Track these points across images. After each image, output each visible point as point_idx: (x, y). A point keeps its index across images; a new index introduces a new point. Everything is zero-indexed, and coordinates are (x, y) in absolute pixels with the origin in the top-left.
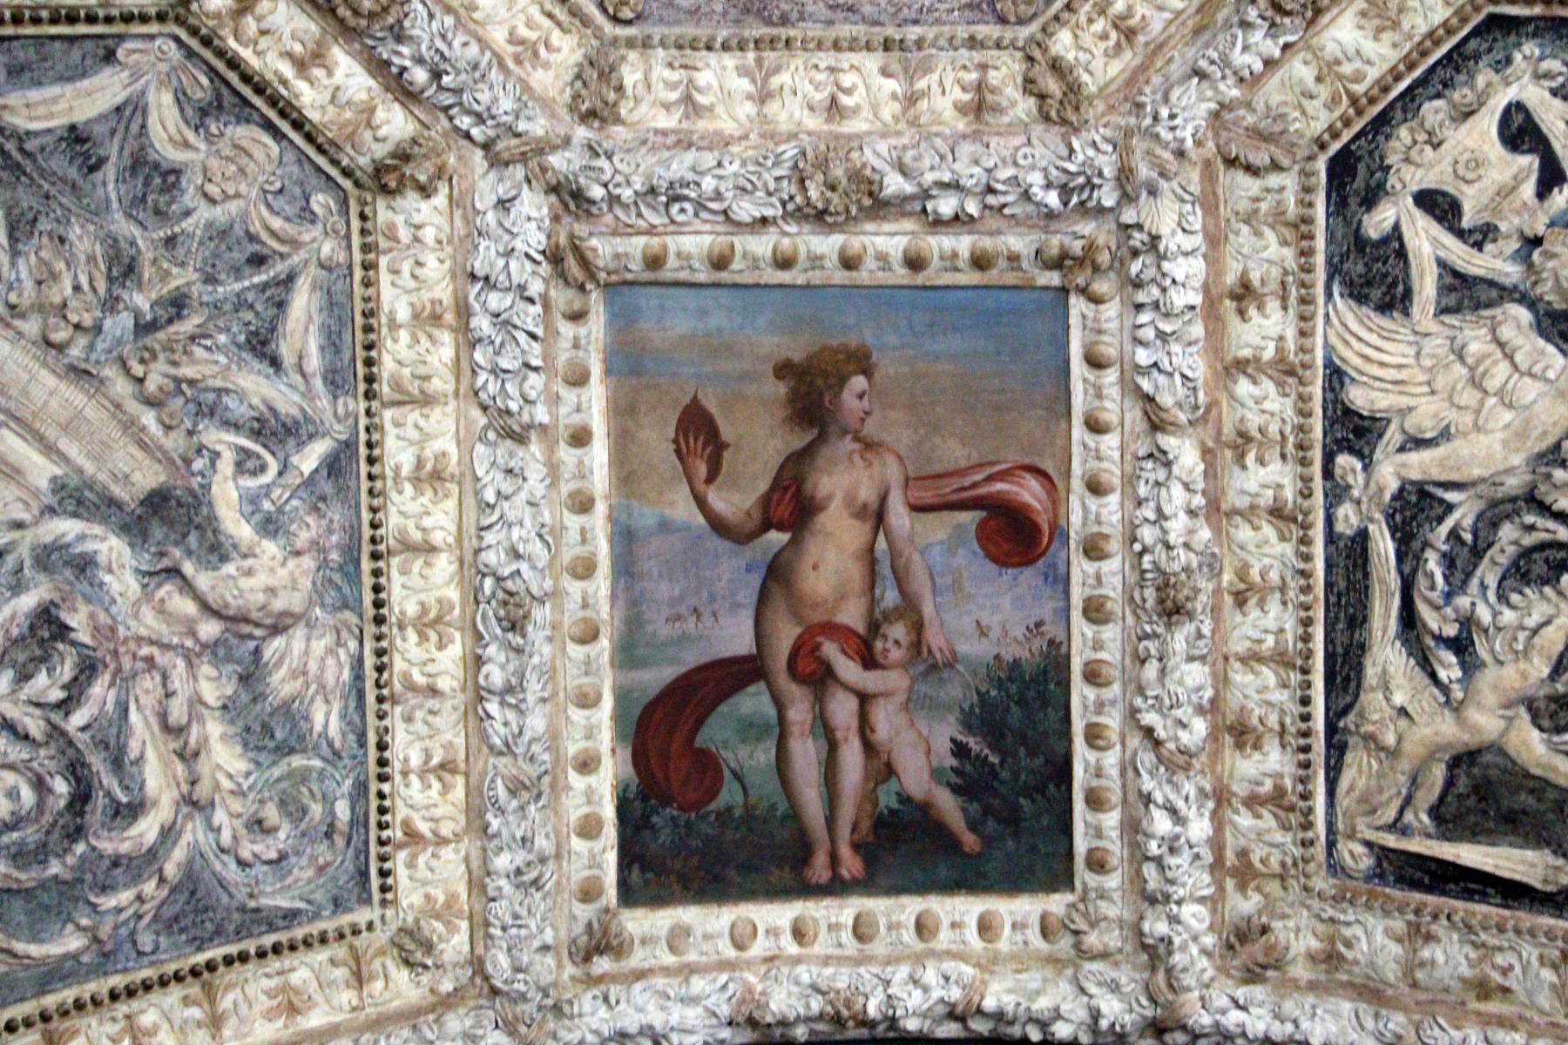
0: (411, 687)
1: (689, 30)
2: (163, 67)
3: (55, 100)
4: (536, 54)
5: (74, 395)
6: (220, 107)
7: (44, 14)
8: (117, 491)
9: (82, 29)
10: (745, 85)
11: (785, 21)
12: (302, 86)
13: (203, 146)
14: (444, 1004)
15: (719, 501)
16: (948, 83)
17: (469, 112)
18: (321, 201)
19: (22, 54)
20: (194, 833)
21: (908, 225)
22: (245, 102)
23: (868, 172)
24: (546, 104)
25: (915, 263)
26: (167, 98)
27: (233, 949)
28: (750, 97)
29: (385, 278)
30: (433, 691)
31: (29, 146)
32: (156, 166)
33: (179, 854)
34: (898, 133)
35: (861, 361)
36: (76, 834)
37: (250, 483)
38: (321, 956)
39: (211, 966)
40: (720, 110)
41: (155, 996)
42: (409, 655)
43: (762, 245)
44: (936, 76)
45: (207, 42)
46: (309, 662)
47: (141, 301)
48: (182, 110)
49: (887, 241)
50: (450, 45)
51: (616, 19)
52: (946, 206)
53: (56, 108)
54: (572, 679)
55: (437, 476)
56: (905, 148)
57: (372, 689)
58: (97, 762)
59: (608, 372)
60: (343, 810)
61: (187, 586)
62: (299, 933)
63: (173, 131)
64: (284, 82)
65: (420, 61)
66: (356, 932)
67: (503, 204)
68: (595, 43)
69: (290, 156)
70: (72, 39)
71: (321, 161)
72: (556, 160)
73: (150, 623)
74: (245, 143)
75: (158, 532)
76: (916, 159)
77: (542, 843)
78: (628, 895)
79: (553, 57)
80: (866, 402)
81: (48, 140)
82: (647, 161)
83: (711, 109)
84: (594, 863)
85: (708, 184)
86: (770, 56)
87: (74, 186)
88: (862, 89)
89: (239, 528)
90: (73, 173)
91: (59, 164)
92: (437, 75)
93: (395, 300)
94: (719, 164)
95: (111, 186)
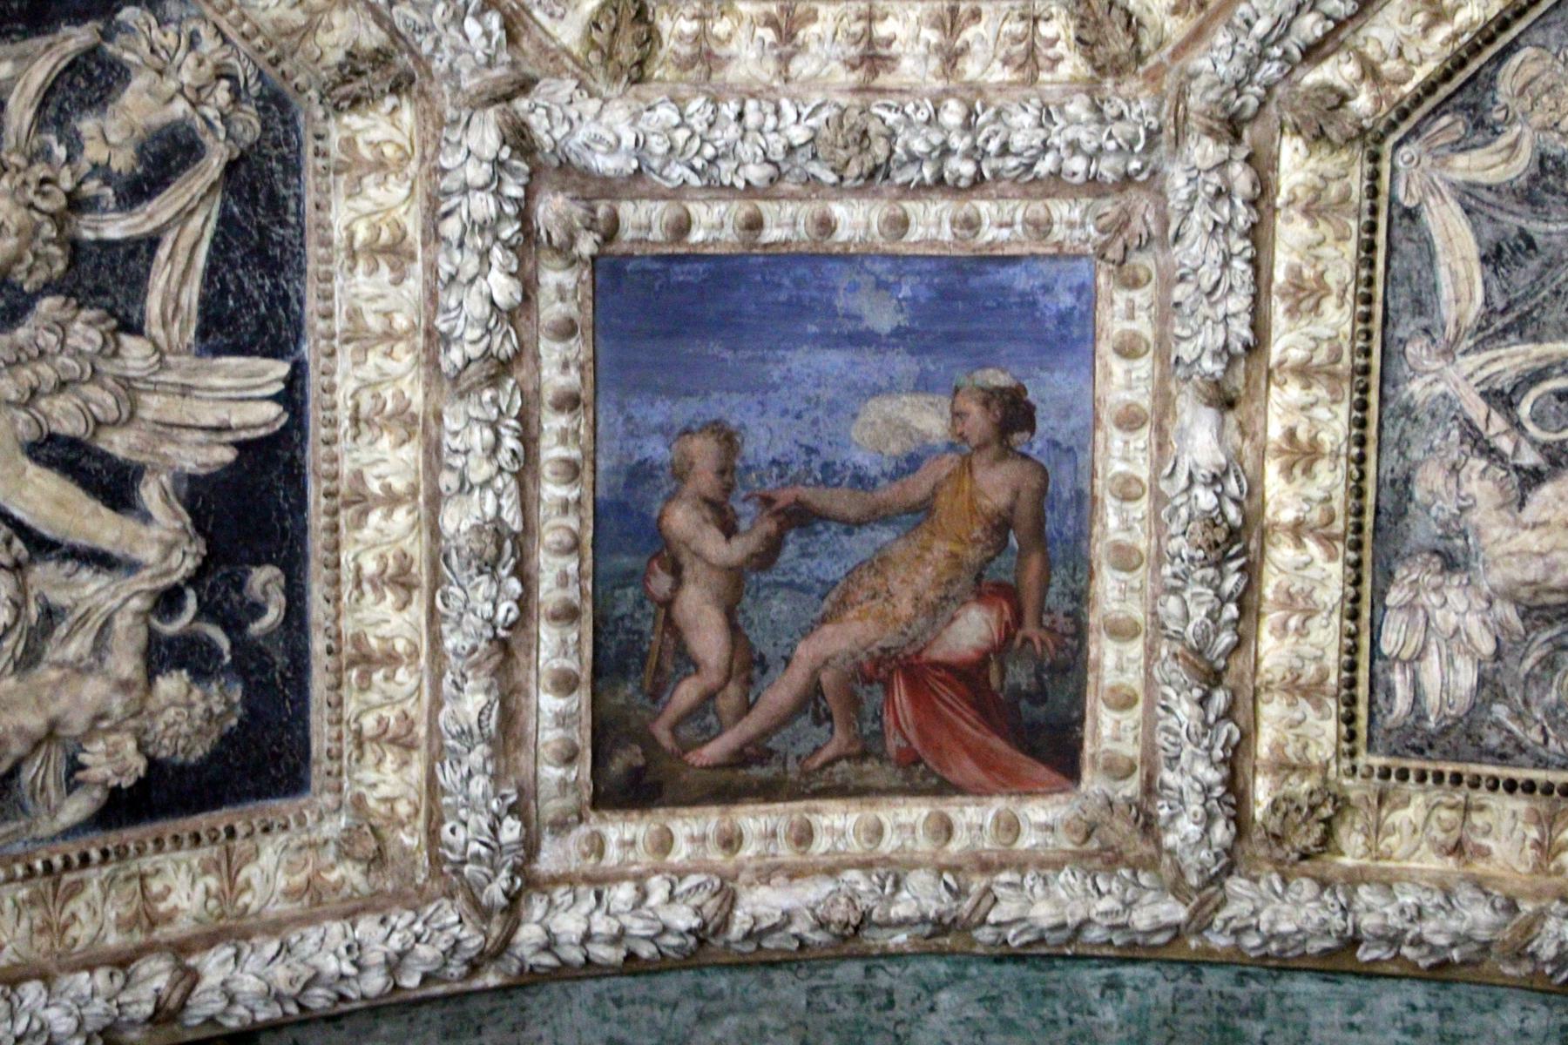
2: (1427, 161)
3: (1454, 274)
6: (1475, 107)
7: (1364, 273)
9: (1381, 238)
12: (1461, 18)
13: (1517, 129)
19: (1402, 298)
22: (1473, 78)
26: (1461, 161)
31: (1500, 305)
32: (1534, 179)
45: (1404, 114)
48: (1474, 147)
53: (1462, 273)
63: (1497, 158)
64: (1455, 36)
69: (1538, 36)
70: (1390, 249)
74: (1519, 84)
81: (1494, 284)
87: (1549, 265)
90: (1534, 264)
95: (1552, 228)
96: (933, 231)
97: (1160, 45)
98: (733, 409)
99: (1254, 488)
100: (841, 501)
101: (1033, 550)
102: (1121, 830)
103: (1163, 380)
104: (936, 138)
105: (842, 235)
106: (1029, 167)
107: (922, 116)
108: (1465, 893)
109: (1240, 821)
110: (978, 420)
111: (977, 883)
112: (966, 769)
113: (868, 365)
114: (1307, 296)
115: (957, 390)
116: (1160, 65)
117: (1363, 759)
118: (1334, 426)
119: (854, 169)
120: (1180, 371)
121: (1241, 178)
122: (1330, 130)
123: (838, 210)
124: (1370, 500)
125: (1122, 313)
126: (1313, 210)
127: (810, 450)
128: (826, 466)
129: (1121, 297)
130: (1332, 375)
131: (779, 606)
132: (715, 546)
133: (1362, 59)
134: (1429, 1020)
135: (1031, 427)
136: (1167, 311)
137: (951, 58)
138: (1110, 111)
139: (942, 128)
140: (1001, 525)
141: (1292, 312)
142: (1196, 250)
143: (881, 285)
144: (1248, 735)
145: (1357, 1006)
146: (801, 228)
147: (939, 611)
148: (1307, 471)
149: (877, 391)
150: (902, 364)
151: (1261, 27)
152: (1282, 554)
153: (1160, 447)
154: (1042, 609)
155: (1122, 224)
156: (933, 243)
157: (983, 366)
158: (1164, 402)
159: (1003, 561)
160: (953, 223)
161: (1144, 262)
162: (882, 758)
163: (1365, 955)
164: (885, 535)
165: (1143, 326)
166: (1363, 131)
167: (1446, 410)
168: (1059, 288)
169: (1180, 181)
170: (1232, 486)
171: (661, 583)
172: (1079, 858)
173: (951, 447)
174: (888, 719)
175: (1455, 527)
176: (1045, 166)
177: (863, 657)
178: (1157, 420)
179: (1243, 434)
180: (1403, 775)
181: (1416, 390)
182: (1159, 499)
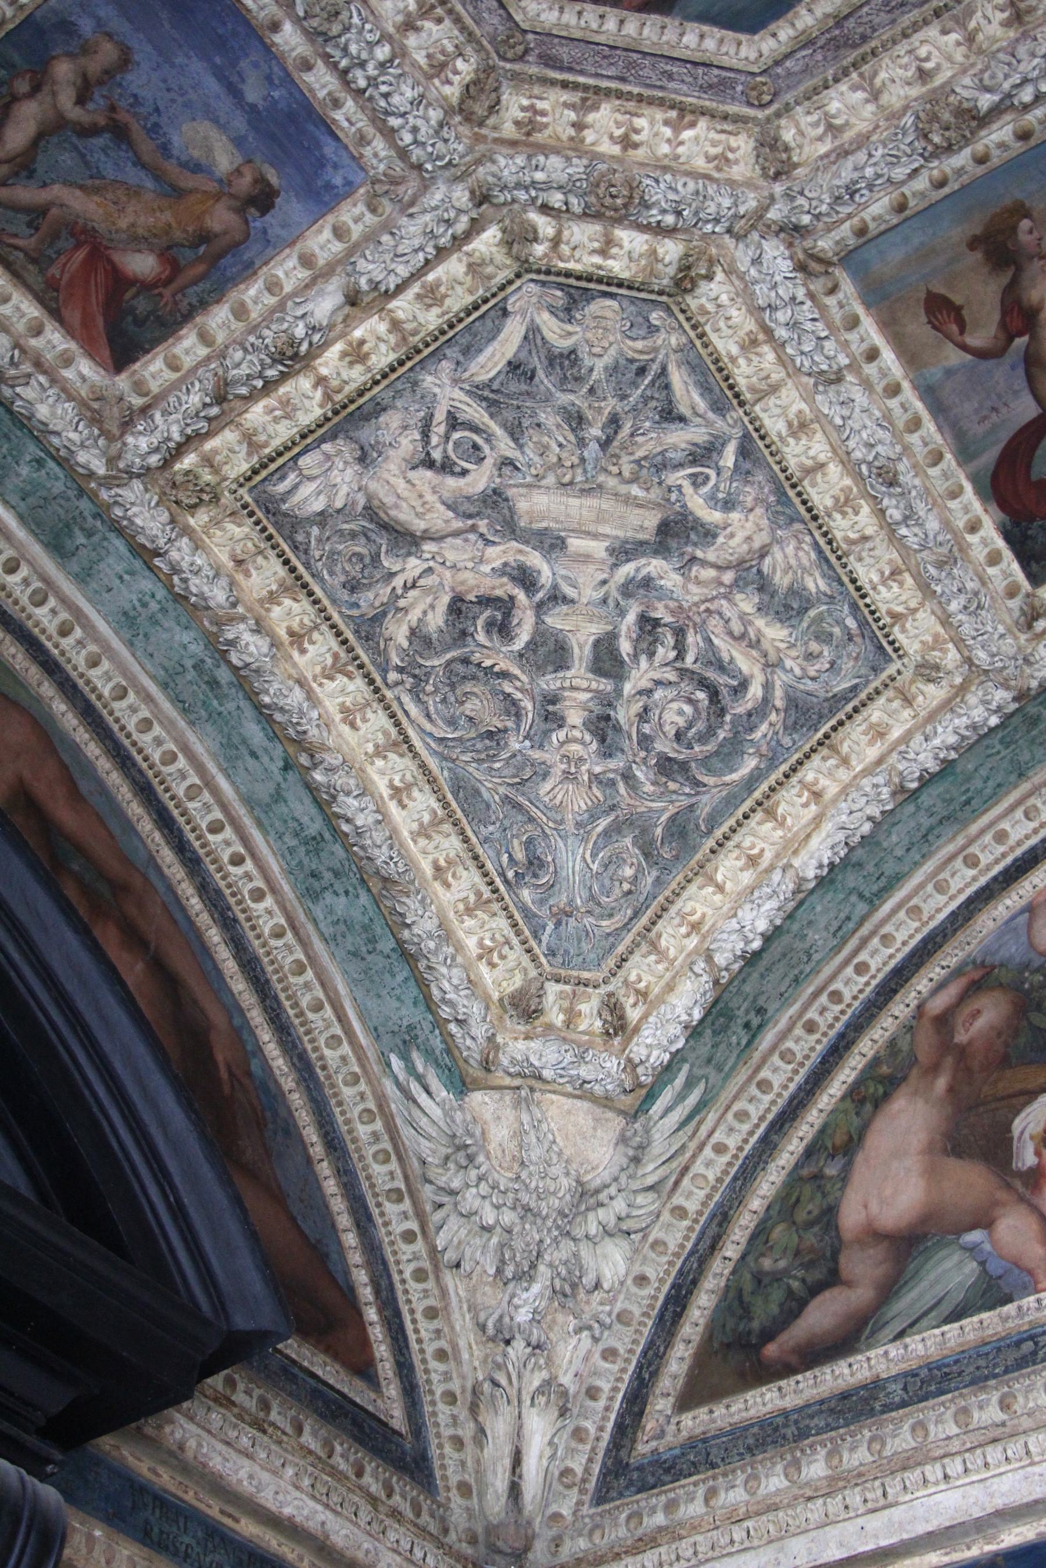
0: (852, 542)
1: (809, 84)
2: (534, 300)
3: (493, 355)
4: (727, 160)
5: (591, 502)
8: (641, 536)
9: (484, 308)
10: (860, 95)
11: (864, 38)
12: (610, 263)
14: (962, 689)
15: (976, 339)
16: (989, 13)
17: (708, 221)
18: (656, 317)
19: (463, 341)
20: (780, 679)
21: (1008, 117)
23: (965, 105)
24: (749, 184)
25: (1024, 135)
26: (546, 315)
27: (833, 722)
28: (867, 101)
29: (713, 337)
30: (865, 538)
31: (495, 387)
32: (561, 355)
33: (779, 693)
34: (973, 65)
35: (1020, 211)
36: (722, 712)
37: (705, 490)
38: (881, 701)
39: (827, 736)
40: (853, 120)
41: (807, 765)
42: (841, 527)
43: (921, 183)
44: (979, 14)
45: (548, 272)
46: (791, 561)
47: (596, 431)
49: (999, 134)
50: (676, 191)
51: (762, 106)
52: (1027, 95)
54: (941, 487)
55: (803, 426)
56: (982, 71)
57: (831, 556)
58: (711, 674)
59: (867, 305)
60: (851, 623)
61: (704, 563)
62: (863, 696)
64: (600, 268)
65: (664, 212)
66: (893, 679)
67: (756, 261)
68: (757, 129)
69: (626, 303)
70: (482, 317)
71: (643, 295)
72: (772, 215)
73: (696, 593)
75: (673, 544)
76: (993, 77)
77: (970, 585)
78: (1035, 580)
79: (738, 154)
80: (1036, 234)
81: (502, 376)
82: (824, 179)
83: (847, 123)
84: (1007, 575)
85: (869, 172)
86: (865, 68)
88: (936, 53)
89: (713, 516)
90: (524, 387)
91: (514, 387)
92: (679, 213)
93: (726, 345)
94: (870, 155)
96: (317, 86)
97: (495, 128)
98: (143, 51)
99: (326, 345)
100: (146, 147)
101: (206, 264)
102: (113, 416)
103: (339, 262)
104: (364, 55)
105: (277, 38)
106: (387, 113)
107: (369, 37)
108: (224, 582)
109: (166, 464)
110: (245, 184)
111: (27, 367)
112: (74, 317)
113: (224, 105)
114: (432, 296)
115: (250, 161)
116: (485, 137)
117: (241, 491)
118: (382, 358)
119: (315, 23)
120: (349, 268)
121: (462, 224)
122: (515, 246)
123: (288, 27)
124: (361, 401)
125: (353, 214)
126: (473, 268)
127: (157, 110)
128: (156, 125)
129: (361, 208)
130: (404, 339)
131: (67, 159)
132: (66, 100)
133: (559, 233)
134: (154, 606)
135: (263, 214)
136: (371, 238)
137: (409, 25)
138: (445, 133)
139: (371, 52)
140: (204, 237)
141: (419, 297)
142: (412, 229)
143: (269, 78)
144: (209, 435)
145: (132, 573)
146: (262, 14)
147: (137, 241)
148: (351, 364)
149: (216, 121)
150: (240, 123)
151: (539, 176)
152: (304, 383)
153: (307, 286)
154: (182, 290)
155: (395, 182)
156: (311, 90)
157: (272, 165)
158: (327, 272)
159: (189, 254)
160: (329, 94)
161: (387, 207)
162: (41, 271)
163: (157, 562)
164: (149, 184)
165: (357, 231)
166: (527, 261)
167: (429, 402)
168: (341, 172)
169: (438, 196)
170: (316, 337)
171: (22, 86)
172: (83, 404)
173: (220, 181)
174: (63, 259)
175: (379, 448)
176: (394, 122)
177: (81, 221)
178: (320, 275)
179: (344, 321)
180: (251, 514)
181: (428, 380)
182: (281, 306)
